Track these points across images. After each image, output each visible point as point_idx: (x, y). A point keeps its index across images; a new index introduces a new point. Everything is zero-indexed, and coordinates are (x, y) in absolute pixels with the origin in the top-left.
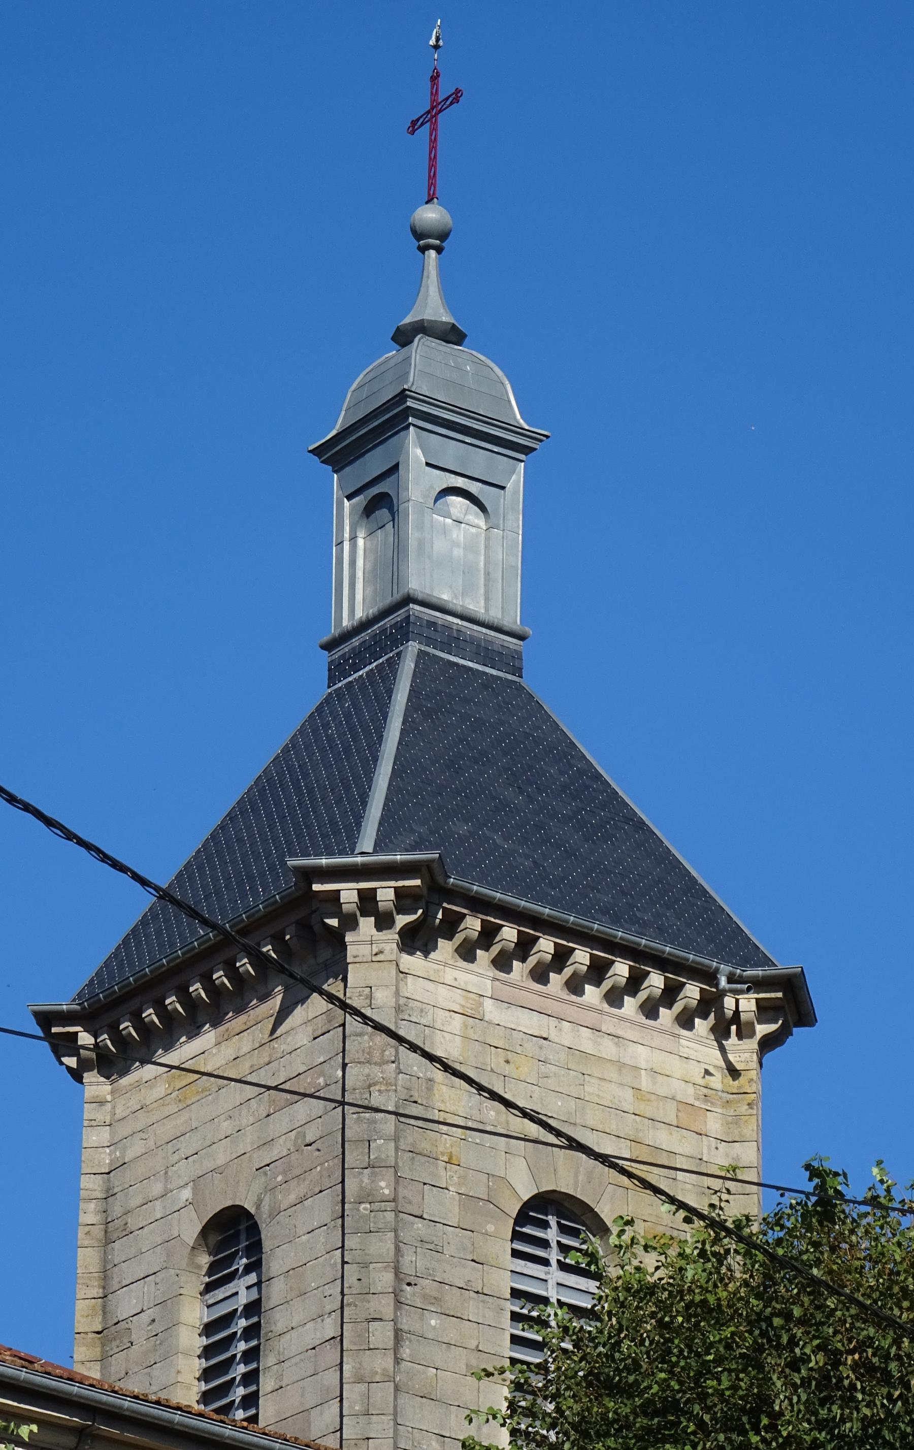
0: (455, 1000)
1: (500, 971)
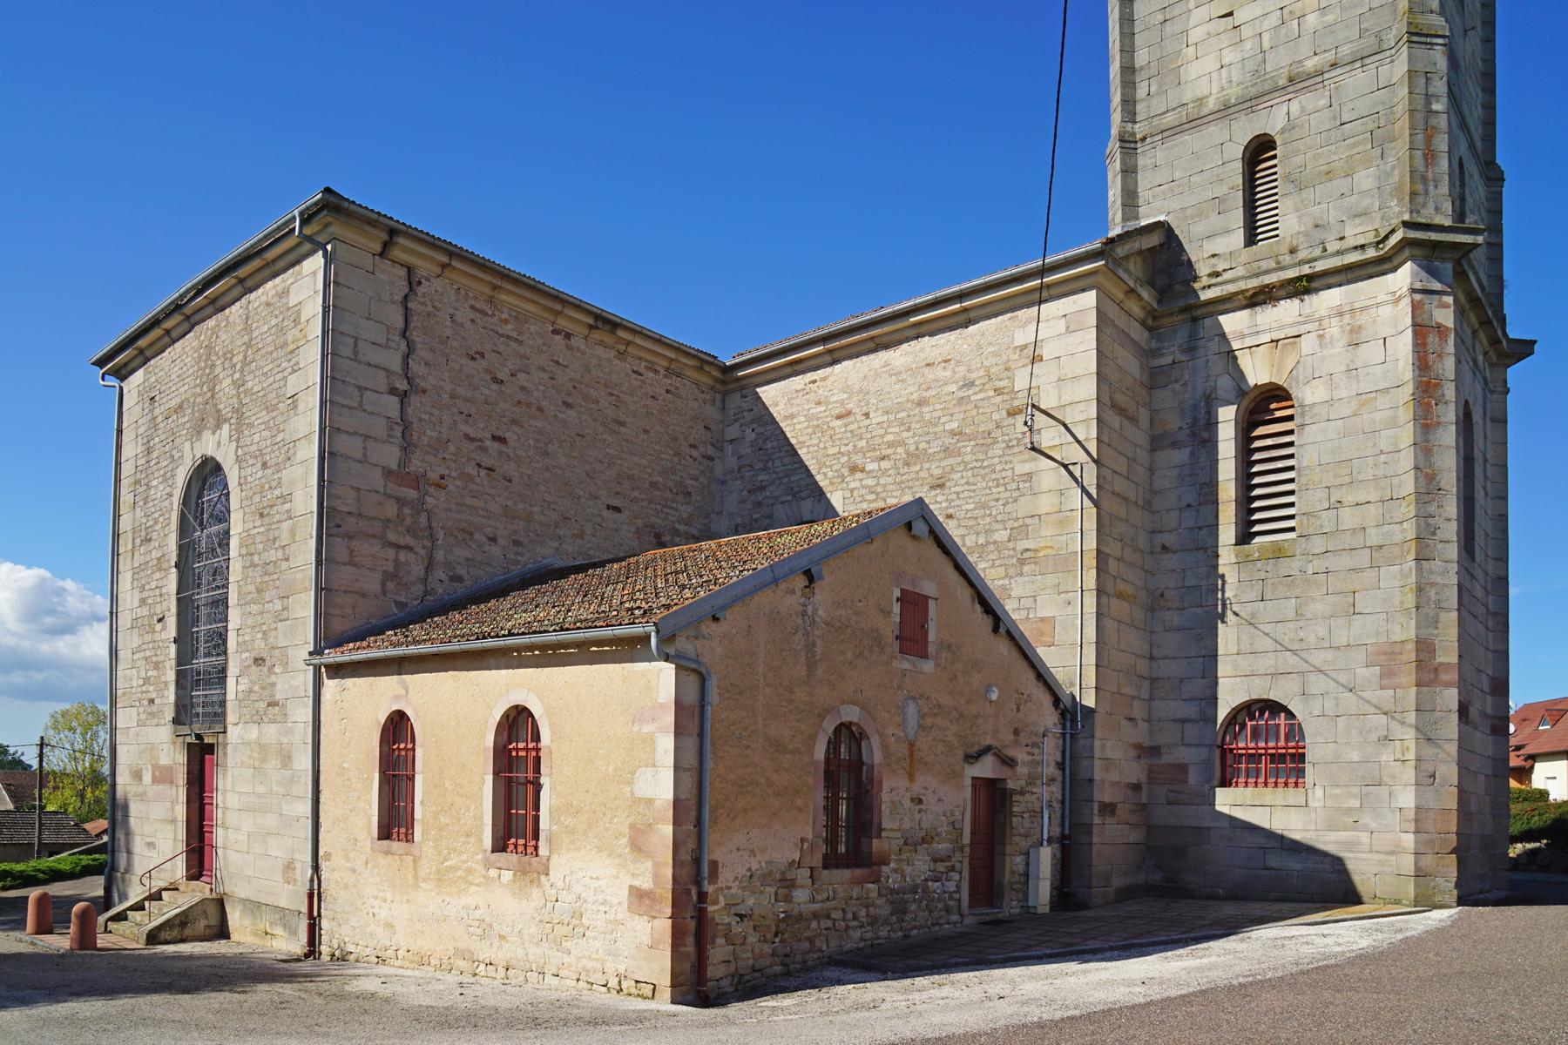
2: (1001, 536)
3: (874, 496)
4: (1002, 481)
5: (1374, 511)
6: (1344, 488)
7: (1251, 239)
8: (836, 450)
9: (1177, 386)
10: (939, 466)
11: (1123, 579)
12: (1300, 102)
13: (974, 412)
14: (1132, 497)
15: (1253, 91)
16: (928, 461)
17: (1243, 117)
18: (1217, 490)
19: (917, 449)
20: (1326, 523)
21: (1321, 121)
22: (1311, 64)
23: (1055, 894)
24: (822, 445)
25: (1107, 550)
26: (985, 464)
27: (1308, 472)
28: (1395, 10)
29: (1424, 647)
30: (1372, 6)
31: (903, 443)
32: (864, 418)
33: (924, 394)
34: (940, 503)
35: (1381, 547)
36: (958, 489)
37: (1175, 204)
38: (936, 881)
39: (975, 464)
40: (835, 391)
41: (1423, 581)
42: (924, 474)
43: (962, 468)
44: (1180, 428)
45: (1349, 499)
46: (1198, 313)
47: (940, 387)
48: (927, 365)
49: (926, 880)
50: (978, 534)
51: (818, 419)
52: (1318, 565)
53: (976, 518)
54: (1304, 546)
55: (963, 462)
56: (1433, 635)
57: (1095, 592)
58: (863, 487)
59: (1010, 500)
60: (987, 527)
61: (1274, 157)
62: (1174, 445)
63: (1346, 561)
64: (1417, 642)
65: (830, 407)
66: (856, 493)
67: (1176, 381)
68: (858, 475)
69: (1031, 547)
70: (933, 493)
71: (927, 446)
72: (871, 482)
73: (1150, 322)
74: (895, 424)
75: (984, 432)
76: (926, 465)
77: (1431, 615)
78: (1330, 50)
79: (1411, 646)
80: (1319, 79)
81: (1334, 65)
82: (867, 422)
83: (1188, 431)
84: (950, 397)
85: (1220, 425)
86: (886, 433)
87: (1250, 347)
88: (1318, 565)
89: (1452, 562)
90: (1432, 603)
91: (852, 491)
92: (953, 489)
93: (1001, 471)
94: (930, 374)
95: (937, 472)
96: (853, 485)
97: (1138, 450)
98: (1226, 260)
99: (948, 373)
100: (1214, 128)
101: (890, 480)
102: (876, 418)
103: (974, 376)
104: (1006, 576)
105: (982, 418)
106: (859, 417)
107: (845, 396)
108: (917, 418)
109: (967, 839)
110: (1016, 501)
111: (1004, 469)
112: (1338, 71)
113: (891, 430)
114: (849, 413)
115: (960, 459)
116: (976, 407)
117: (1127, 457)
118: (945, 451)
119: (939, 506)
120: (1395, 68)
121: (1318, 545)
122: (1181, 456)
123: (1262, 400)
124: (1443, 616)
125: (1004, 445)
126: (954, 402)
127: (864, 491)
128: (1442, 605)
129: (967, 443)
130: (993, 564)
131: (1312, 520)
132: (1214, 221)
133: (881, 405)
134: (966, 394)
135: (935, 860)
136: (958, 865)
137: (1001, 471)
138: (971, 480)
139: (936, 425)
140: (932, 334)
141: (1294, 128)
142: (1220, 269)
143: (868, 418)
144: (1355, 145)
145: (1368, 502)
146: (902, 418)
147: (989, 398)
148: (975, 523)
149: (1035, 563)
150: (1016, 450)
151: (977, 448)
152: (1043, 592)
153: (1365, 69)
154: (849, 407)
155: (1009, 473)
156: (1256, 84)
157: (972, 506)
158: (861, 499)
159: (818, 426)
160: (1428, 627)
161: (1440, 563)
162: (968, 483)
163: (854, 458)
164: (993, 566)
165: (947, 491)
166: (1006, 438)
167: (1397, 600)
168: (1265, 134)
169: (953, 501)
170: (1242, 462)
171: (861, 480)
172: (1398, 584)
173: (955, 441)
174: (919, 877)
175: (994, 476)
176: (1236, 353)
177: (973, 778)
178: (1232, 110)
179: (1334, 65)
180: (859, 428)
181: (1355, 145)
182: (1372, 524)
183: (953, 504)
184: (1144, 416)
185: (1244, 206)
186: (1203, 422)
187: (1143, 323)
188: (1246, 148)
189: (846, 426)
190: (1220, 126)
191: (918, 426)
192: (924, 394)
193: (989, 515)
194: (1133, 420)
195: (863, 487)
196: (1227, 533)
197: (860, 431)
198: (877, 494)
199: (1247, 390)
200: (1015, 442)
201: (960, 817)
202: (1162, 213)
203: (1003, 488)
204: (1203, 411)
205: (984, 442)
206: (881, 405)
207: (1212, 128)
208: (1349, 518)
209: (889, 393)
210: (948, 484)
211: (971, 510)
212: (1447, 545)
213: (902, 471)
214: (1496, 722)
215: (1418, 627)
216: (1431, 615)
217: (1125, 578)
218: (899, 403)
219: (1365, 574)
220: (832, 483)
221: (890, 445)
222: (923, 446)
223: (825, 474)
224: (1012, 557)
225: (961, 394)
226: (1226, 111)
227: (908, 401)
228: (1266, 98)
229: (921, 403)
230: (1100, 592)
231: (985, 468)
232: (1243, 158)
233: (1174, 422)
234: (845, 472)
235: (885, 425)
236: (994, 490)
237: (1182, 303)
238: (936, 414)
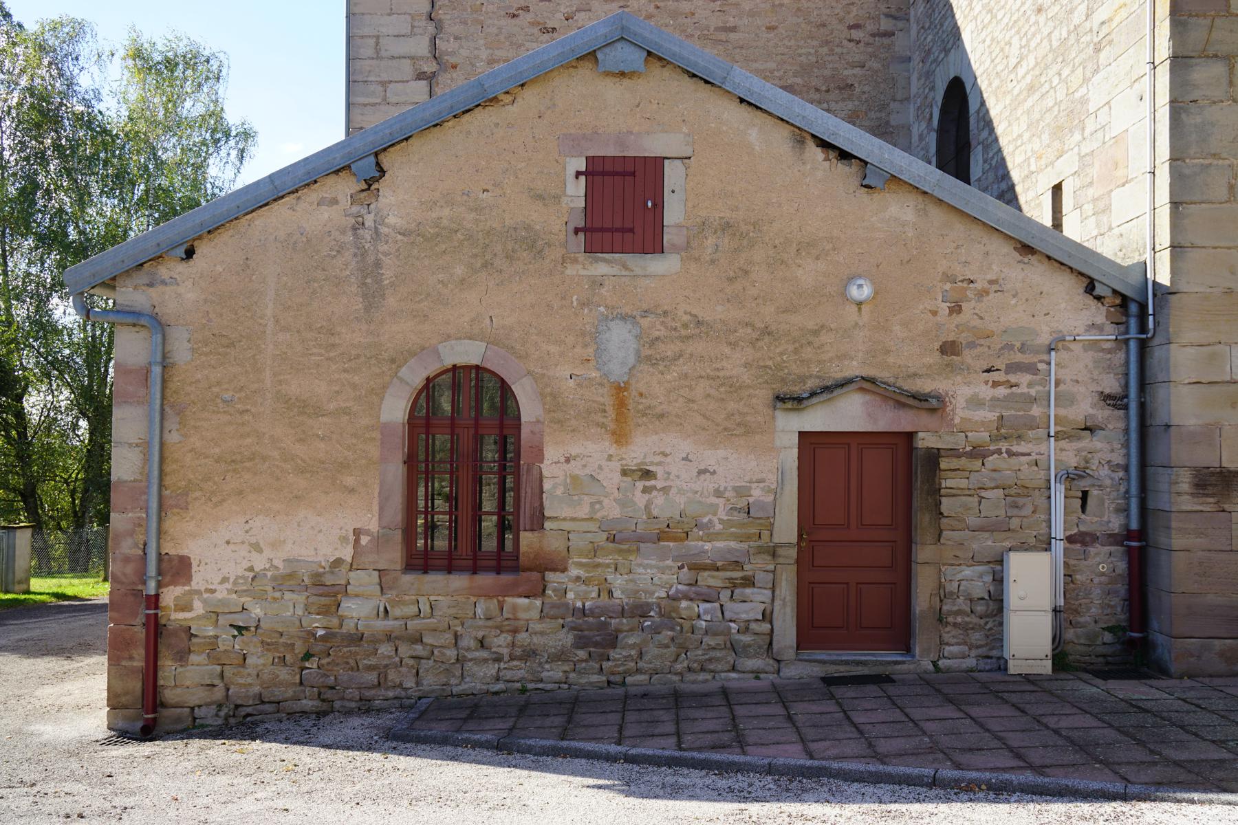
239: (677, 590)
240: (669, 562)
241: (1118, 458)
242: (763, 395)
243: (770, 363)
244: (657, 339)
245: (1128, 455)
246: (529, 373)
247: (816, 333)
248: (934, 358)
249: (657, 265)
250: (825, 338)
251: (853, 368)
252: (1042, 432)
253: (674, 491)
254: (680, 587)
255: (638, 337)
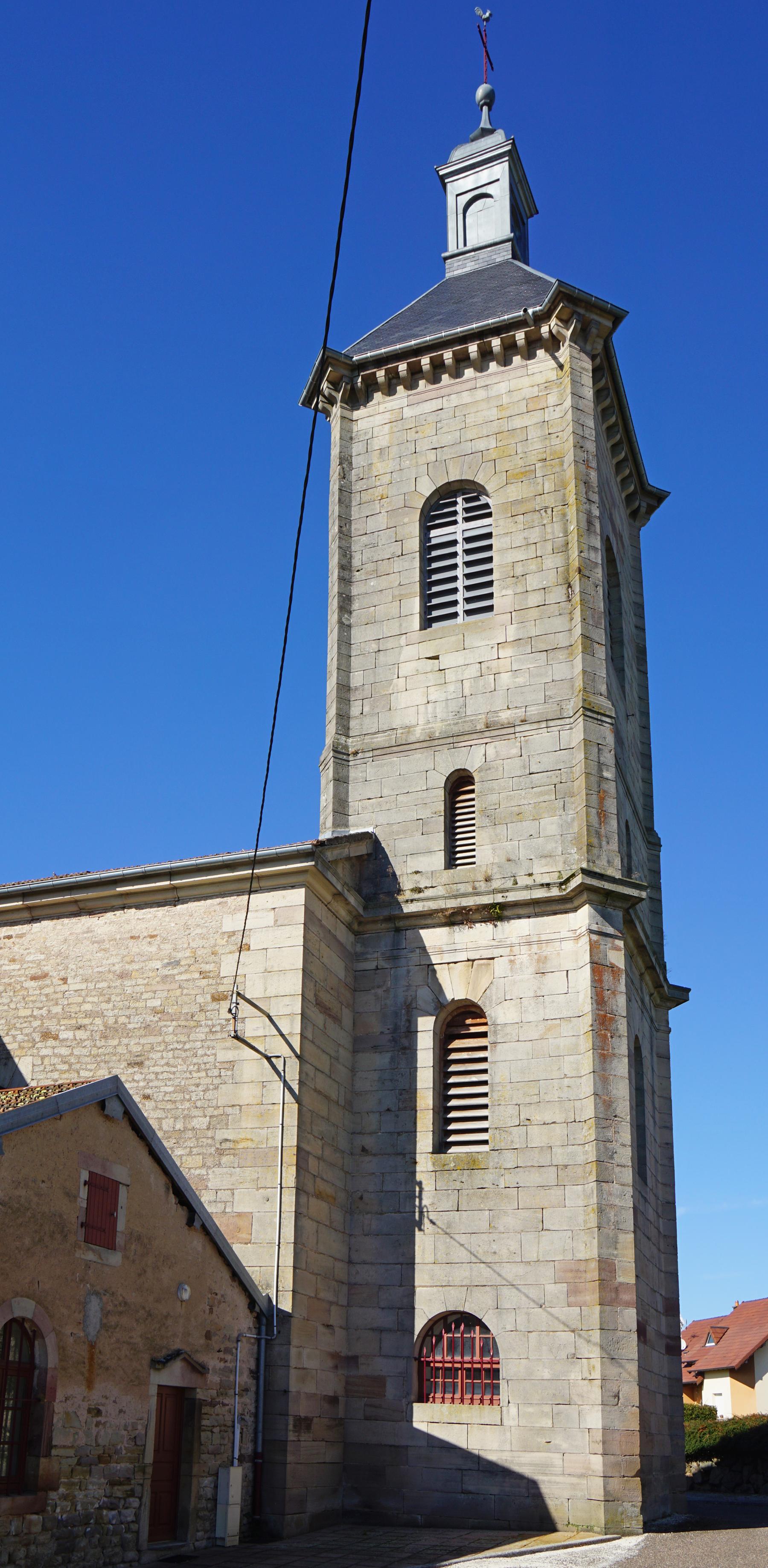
0: (387, 417)
1: (411, 390)
2: (200, 1122)
3: (66, 1067)
4: (203, 1066)
5: (559, 1131)
6: (533, 1106)
7: (451, 862)
8: (28, 1012)
9: (380, 991)
10: (139, 1044)
11: (322, 1179)
12: (495, 747)
13: (178, 992)
14: (334, 1096)
15: (456, 729)
16: (128, 1036)
17: (446, 751)
18: (415, 1097)
19: (116, 1022)
20: (516, 1140)
21: (514, 767)
22: (505, 716)
23: (245, 1521)
24: (13, 1006)
25: (308, 1148)
26: (187, 1046)
27: (500, 1088)
28: (573, 686)
29: (606, 1266)
30: (555, 678)
31: (101, 1014)
32: (61, 982)
33: (127, 967)
34: (138, 1082)
35: (566, 1166)
36: (157, 1069)
37: (382, 819)
38: (112, 1509)
39: (176, 1045)
40: (32, 951)
41: (604, 1202)
42: (120, 1050)
43: (162, 1048)
44: (382, 1033)
45: (537, 1117)
46: (400, 924)
47: (144, 961)
48: (132, 937)
49: (100, 1508)
50: (176, 1118)
51: (11, 977)
52: (509, 1179)
53: (175, 1102)
54: (496, 1160)
55: (164, 1041)
56: (613, 1255)
57: (294, 1190)
58: (55, 1055)
59: (211, 1087)
60: (186, 1112)
61: (472, 791)
62: (375, 1048)
63: (534, 1178)
64: (599, 1261)
65: (25, 966)
66: (46, 1061)
67: (379, 987)
68: (51, 1042)
69: (229, 1138)
70: (131, 1070)
71: (127, 1021)
72: (64, 1051)
73: (356, 927)
74: (94, 993)
75: (187, 1014)
76: (125, 1041)
77: (611, 1235)
78: (520, 708)
79: (594, 1265)
80: (511, 730)
81: (524, 721)
82: (65, 987)
83: (389, 1037)
84: (154, 974)
85: (419, 1034)
86: (84, 1002)
87: (448, 963)
88: (509, 1179)
89: (628, 1185)
90: (611, 1224)
91: (43, 1058)
92: (152, 1069)
93: (202, 1056)
94: (134, 948)
95: (136, 1049)
96: (44, 1052)
97: (341, 1050)
98: (427, 878)
99: (153, 949)
100: (420, 755)
101: (85, 1051)
102: (74, 984)
103: (179, 955)
104: (204, 1166)
105: (185, 998)
106: (56, 981)
107: (42, 957)
108: (118, 991)
109: (149, 1458)
110: (216, 1088)
111: (206, 1054)
112: (527, 727)
113: (90, 999)
114: (45, 976)
115: (160, 1039)
116: (180, 987)
117: (331, 1056)
118: (145, 1028)
119: (135, 1084)
120: (574, 735)
121: (509, 1159)
122: (382, 1060)
123: (457, 1016)
124: (622, 1237)
125: (207, 1030)
126: (158, 979)
127: (55, 1060)
128: (621, 1227)
129: (169, 1023)
130: (191, 1152)
131: (504, 1135)
132: (416, 841)
133: (81, 971)
134: (170, 972)
135: (112, 1484)
136: (138, 1489)
137: (202, 1056)
138: (172, 1061)
139: (138, 1000)
140: (138, 907)
141: (490, 769)
142: (422, 886)
143: (65, 983)
144: (541, 794)
145: (554, 1123)
146: (103, 989)
147: (194, 980)
148: (173, 1107)
149: (234, 1155)
150: (219, 1036)
151: (180, 1030)
152: (241, 1186)
153: (549, 730)
154: (46, 969)
155: (211, 1059)
156: (457, 723)
157: (171, 1089)
158: (51, 1068)
159: (10, 985)
160: (608, 1248)
161: (617, 1186)
162: (167, 1064)
163: (47, 1023)
164: (190, 1154)
165: (145, 1070)
166: (210, 1023)
167: (581, 1218)
168: (465, 770)
169: (151, 1081)
170: (440, 1073)
171: (54, 1048)
172: (581, 1203)
173: (156, 1019)
174: (92, 1504)
175: (195, 1060)
176: (436, 967)
177: (159, 1386)
178: (436, 742)
179: (524, 721)
180: (55, 992)
181: (541, 794)
182: (558, 1143)
183: (151, 1084)
184: (347, 1017)
185: (445, 831)
186: (403, 1029)
187: (349, 927)
188: (448, 779)
189: (41, 989)
190: (425, 754)
191: (118, 999)
192: (127, 967)
193: (189, 1100)
194: (337, 1019)
195: (55, 1055)
196: (425, 1141)
197: (56, 996)
198: (70, 1065)
199: (445, 1003)
200: (218, 1028)
201: (143, 1432)
202: (371, 825)
203: (203, 1074)
204: (404, 1019)
205: (187, 1024)
206: (81, 971)
207: (417, 755)
208: (538, 1136)
209: (90, 960)
210: (147, 1063)
211: (170, 1093)
212: (623, 1169)
213: (98, 1043)
214: (668, 1340)
215: (600, 1247)
216: (611, 1235)
217: (325, 1178)
218: (100, 972)
219: (552, 1191)
220: (21, 1048)
221: (88, 1015)
222: (122, 1020)
223: (14, 1037)
224: (211, 1146)
225: (166, 972)
226: (431, 742)
227: (110, 971)
228: (466, 738)
229: (123, 975)
230: (300, 1190)
231: (186, 1051)
232: (445, 787)
233: (376, 1026)
234: (37, 1037)
235: (83, 993)
236: (195, 1075)
237: (386, 913)
238: (137, 989)
239: (104, 1502)
240: (102, 1480)
241: (253, 1410)
242: (146, 1358)
243: (149, 1336)
244: (109, 1311)
245: (257, 1408)
246: (54, 1329)
247: (166, 1317)
248: (202, 1341)
249: (115, 1259)
250: (169, 1322)
251: (177, 1345)
252: (231, 1392)
253: (108, 1425)
254: (105, 1499)
255: (102, 1309)
